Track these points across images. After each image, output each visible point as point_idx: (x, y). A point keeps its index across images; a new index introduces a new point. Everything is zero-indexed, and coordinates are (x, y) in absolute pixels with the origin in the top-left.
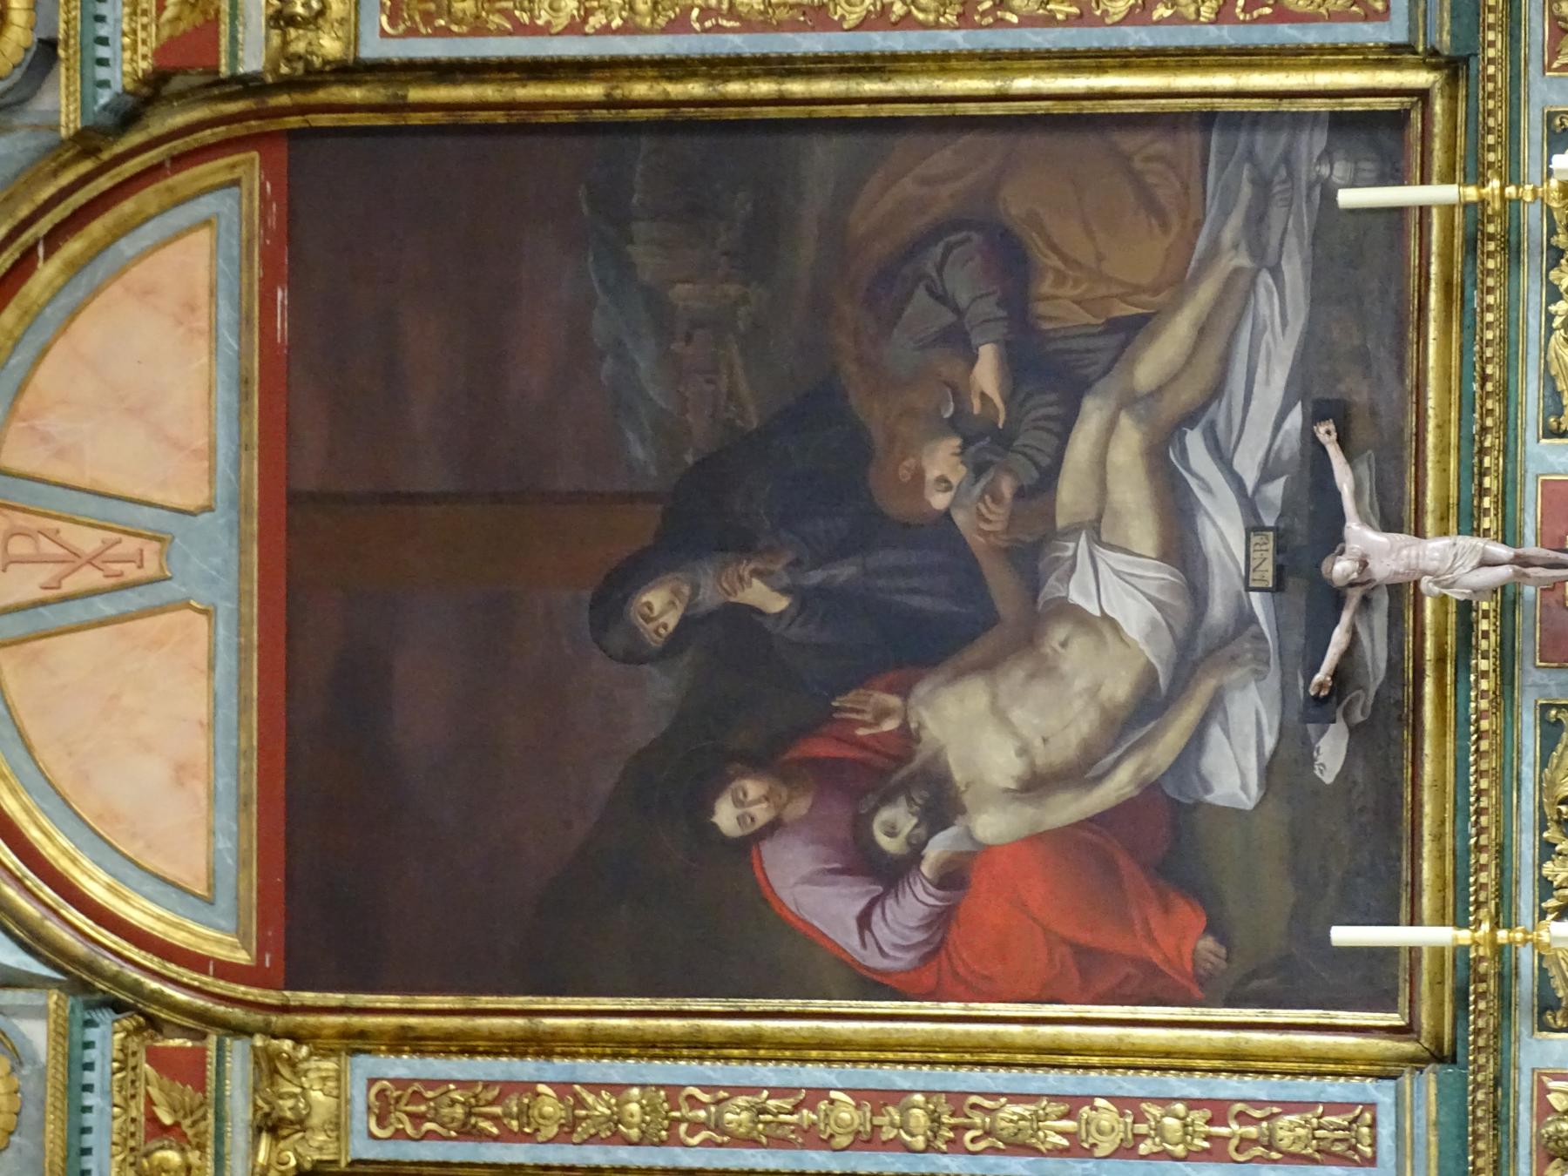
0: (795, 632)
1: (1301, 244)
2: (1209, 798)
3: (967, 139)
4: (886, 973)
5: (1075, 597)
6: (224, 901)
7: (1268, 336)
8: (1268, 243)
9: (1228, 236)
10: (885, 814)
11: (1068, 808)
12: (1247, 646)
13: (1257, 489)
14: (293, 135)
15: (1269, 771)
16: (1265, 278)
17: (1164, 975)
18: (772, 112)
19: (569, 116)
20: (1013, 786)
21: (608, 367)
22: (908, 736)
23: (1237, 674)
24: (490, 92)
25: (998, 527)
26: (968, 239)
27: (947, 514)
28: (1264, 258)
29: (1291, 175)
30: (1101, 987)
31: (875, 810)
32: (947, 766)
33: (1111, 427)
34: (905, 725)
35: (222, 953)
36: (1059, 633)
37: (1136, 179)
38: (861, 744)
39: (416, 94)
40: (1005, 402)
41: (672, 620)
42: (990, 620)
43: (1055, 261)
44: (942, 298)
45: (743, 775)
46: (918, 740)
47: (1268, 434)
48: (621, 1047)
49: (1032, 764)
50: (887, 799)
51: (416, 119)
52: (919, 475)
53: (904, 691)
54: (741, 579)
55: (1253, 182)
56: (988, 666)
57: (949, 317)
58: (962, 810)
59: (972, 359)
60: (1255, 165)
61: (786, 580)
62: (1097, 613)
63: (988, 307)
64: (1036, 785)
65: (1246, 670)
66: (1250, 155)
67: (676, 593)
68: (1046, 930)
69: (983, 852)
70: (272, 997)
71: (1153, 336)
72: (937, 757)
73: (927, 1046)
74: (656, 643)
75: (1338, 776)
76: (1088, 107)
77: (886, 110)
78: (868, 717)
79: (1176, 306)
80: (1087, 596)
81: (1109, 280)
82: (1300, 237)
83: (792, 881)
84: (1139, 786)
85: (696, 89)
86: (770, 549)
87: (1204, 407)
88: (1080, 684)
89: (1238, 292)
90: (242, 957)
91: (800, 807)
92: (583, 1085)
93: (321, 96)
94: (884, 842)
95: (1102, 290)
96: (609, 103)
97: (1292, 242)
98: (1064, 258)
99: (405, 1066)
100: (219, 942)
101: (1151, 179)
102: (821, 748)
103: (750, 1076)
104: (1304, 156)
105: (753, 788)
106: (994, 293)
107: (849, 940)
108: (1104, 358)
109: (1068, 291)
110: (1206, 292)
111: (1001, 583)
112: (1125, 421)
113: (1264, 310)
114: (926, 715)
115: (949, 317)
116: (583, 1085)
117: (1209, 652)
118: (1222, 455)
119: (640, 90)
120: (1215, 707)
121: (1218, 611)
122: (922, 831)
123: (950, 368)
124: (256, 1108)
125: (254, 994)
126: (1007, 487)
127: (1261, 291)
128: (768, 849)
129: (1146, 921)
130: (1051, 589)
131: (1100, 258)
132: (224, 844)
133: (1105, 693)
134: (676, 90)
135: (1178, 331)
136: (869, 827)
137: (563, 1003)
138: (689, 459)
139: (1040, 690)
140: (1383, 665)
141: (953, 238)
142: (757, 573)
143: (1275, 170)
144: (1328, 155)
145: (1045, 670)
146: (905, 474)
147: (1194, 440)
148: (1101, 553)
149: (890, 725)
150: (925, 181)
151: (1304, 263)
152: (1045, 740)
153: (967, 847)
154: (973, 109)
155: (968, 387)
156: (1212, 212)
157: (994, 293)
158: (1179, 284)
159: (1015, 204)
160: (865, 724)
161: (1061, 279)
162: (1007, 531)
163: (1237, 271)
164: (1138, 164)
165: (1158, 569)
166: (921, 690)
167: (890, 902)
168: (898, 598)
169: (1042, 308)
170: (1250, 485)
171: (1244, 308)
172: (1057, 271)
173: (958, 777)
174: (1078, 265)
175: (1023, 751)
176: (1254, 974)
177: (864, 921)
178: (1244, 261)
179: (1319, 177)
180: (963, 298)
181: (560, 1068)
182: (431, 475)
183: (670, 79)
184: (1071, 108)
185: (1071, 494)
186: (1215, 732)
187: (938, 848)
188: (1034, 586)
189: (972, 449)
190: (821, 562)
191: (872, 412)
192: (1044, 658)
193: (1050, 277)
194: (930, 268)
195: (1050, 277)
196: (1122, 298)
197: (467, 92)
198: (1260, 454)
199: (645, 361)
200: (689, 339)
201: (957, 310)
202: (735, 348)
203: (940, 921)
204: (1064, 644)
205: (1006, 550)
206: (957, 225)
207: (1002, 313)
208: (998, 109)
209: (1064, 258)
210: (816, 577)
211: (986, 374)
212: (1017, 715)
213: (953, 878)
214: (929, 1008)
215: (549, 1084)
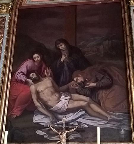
0: (58, 63)
1: (112, 127)
2: (34, 116)
3: (125, 81)
4: (15, 76)
5: (62, 97)
6: (30, 3)
7: (98, 122)
8: (111, 122)
9: (112, 116)
10: (35, 74)
11: (34, 97)
12: (55, 121)
13: (77, 121)
14: (121, 3)
15: (38, 124)
16: (107, 122)
17: (11, 110)
18: (127, 56)
19: (124, 32)
20: (38, 90)
21: (92, 39)
22: (45, 77)
23: (51, 119)
24: (127, 22)
25: (72, 87)
26: (110, 81)
27: (74, 80)
28: (109, 122)
29: (121, 125)
30: (11, 103)
31: (35, 73)
32: (40, 82)
33: (86, 101)
34: (46, 76)
35: (23, 3)
36: (57, 95)
37: (120, 103)
38: (44, 71)
39: (126, 14)
40: (88, 87)
41: (60, 48)
42: (59, 86)
43: (108, 93)
44: (102, 79)
45: (40, 57)
46: (44, 78)
47: (84, 123)
48: (8, 44)
49: (40, 92)
50: (37, 75)
51: (123, 15)
52: (79, 77)
53: (50, 76)
54: (65, 56)
55: (120, 120)
56: (53, 86)
57: (100, 79)
58: (35, 84)
59: (94, 83)
60: (122, 120)
61: (65, 61)
62: (60, 100)
63: (101, 84)
64: (38, 93)
65: (52, 120)
66: (124, 119)
67: (64, 48)
68: (19, 95)
69: (30, 87)
70: (18, 7)
71: (98, 107)
72: (42, 80)
73: (5, 80)
74: (58, 46)
75: (37, 134)
76: (130, 96)
77: (128, 70)
78: (47, 71)
79: (102, 109)
80: (62, 99)
81: (105, 100)
82: (113, 127)
83: (27, 63)
84: (37, 106)
85: (129, 46)
86: (69, 59)
87: (88, 114)
88: (51, 98)
89: (105, 118)
90: (23, 5)
91: (36, 64)
92: (3, 39)
93: (125, 4)
94: (31, 74)
95: (104, 100)
96: (126, 35)
97: (112, 125)
98: (108, 94)
99: (7, 20)
100: (25, 3)
101: (120, 105)
102: (43, 66)
103: (2, 58)
104: (124, 127)
105: (39, 59)
106: (103, 85)
107: (19, 71)
108: (95, 100)
109: (104, 95)
110: (104, 113)
111: (65, 87)
112: (86, 103)
113: (102, 122)
114: (47, 79)
115: (100, 79)
116: (3, 39)
117: (54, 115)
118: (81, 116)
119: (128, 39)
120: (47, 116)
121: (60, 116)
122: (32, 79)
123: (93, 79)
124: (3, 4)
125: (18, 5)
126: (77, 88)
127: (105, 121)
128: (32, 60)
129: (19, 108)
130: (63, 94)
131: (108, 99)
132: (36, 3)
133: (49, 101)
134: (129, 43)
135: (99, 110)
136: (34, 72)
137: (14, 38)
138: (81, 49)
139: (50, 93)
140: (52, 140)
141: (111, 80)
142: (66, 57)
143: (122, 123)
144: (125, 130)
145: (53, 93)
146: (79, 75)
147: (84, 112)
148: (68, 100)
149: (46, 74)
150: (118, 76)
151: (109, 127)
152: (43, 94)
153: (30, 84)
154: (129, 81)
155: (90, 82)
156: (116, 114)
157: (103, 85)
158: (105, 110)
159: (116, 87)
160: (46, 71)
161: (105, 94)
162: (71, 88)
163: (107, 118)
164: (122, 103)
165: (66, 108)
166: (50, 78)
167: (24, 75)
168: (62, 76)
169: (101, 91)
170: (77, 120)
171: (103, 119)
172: (106, 93)
173: (39, 83)
174: (107, 96)
175: (42, 91)
176: (10, 122)
177: (22, 72)
178: (109, 119)
179: (122, 129)
180: (102, 81)
181: (5, 37)
182: (78, 20)
183: (130, 43)
184: (130, 94)
185: (76, 96)
186: (43, 116)
187: (30, 81)
188: (64, 92)
189: (82, 83)
190: (67, 65)
191: (87, 70)
192: (54, 93)
193: (106, 92)
194: (106, 77)
195: (106, 92)
196: (103, 102)
197: (127, 19)
198: (82, 122)
199: (94, 43)
200: (96, 48)
201: (101, 80)
202: (95, 53)
203: (21, 81)
204: (56, 96)
205: (69, 88)
206: (112, 80)
207: (100, 86)
208: (129, 84)
209: (108, 94)
210: (65, 64)
211: (92, 84)
212: (47, 90)
213: (26, 83)
214: (10, 80)
215: (3, 36)
